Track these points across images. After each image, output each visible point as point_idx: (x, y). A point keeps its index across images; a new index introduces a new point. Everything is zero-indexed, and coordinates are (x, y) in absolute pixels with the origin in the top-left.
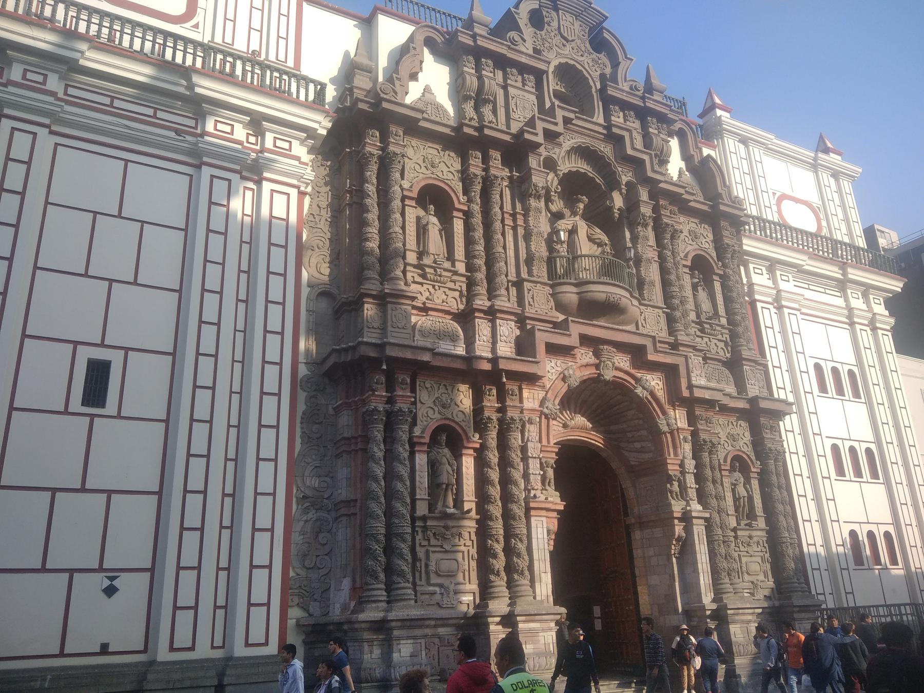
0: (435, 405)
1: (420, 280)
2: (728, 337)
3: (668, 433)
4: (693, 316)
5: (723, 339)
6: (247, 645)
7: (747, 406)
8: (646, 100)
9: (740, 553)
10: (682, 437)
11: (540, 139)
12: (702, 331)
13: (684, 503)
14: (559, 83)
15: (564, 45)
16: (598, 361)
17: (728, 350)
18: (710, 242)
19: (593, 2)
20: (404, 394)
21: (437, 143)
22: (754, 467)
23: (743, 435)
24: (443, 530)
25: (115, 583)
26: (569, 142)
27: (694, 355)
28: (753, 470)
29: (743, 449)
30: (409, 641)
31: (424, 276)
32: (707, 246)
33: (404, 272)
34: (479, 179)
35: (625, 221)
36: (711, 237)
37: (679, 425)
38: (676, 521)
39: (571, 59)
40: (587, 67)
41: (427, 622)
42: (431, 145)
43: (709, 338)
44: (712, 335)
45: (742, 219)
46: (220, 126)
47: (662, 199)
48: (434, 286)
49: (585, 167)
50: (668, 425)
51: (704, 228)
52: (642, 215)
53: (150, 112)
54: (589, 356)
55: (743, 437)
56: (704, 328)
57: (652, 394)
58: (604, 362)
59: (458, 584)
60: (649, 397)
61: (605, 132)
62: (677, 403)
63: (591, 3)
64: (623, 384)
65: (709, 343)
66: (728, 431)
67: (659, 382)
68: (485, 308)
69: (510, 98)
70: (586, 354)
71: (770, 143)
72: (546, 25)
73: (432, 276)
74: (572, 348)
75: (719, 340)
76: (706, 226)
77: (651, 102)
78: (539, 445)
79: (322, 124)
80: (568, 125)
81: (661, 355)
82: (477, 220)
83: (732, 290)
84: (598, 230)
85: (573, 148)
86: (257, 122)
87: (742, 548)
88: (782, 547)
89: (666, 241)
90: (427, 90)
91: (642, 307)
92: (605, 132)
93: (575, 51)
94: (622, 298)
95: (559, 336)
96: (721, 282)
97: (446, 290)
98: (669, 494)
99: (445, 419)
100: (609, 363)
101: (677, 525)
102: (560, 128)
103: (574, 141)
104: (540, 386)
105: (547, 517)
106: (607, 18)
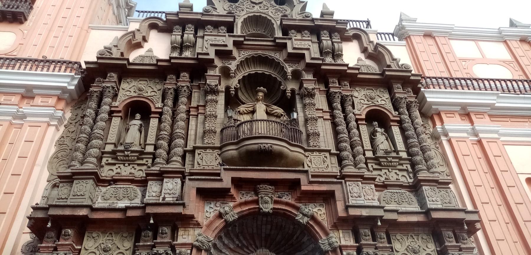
0: (98, 250)
4: (369, 154)
8: (315, 21)
11: (212, 56)
12: (379, 164)
15: (253, 7)
16: (256, 198)
17: (410, 177)
18: (386, 100)
20: (67, 243)
23: (427, 247)
27: (362, 183)
31: (116, 159)
32: (383, 102)
33: (100, 159)
34: (172, 91)
35: (297, 98)
36: (387, 96)
37: (343, 243)
39: (258, 12)
40: (270, 14)
43: (388, 169)
44: (389, 166)
47: (330, 77)
48: (124, 165)
50: (330, 244)
51: (380, 91)
54: (249, 195)
55: (426, 248)
56: (380, 162)
57: (313, 218)
58: (262, 198)
60: (311, 223)
64: (285, 213)
65: (388, 173)
66: (407, 244)
67: (321, 208)
69: (205, 41)
70: (247, 194)
71: (452, 30)
73: (122, 158)
74: (228, 190)
76: (382, 90)
77: (319, 21)
81: (315, 185)
82: (167, 117)
84: (275, 107)
85: (247, 59)
89: (335, 104)
90: (150, 51)
91: (307, 154)
93: (262, 7)
94: (274, 146)
97: (136, 166)
100: (267, 198)
102: (230, 47)
103: (246, 54)
104: (194, 225)
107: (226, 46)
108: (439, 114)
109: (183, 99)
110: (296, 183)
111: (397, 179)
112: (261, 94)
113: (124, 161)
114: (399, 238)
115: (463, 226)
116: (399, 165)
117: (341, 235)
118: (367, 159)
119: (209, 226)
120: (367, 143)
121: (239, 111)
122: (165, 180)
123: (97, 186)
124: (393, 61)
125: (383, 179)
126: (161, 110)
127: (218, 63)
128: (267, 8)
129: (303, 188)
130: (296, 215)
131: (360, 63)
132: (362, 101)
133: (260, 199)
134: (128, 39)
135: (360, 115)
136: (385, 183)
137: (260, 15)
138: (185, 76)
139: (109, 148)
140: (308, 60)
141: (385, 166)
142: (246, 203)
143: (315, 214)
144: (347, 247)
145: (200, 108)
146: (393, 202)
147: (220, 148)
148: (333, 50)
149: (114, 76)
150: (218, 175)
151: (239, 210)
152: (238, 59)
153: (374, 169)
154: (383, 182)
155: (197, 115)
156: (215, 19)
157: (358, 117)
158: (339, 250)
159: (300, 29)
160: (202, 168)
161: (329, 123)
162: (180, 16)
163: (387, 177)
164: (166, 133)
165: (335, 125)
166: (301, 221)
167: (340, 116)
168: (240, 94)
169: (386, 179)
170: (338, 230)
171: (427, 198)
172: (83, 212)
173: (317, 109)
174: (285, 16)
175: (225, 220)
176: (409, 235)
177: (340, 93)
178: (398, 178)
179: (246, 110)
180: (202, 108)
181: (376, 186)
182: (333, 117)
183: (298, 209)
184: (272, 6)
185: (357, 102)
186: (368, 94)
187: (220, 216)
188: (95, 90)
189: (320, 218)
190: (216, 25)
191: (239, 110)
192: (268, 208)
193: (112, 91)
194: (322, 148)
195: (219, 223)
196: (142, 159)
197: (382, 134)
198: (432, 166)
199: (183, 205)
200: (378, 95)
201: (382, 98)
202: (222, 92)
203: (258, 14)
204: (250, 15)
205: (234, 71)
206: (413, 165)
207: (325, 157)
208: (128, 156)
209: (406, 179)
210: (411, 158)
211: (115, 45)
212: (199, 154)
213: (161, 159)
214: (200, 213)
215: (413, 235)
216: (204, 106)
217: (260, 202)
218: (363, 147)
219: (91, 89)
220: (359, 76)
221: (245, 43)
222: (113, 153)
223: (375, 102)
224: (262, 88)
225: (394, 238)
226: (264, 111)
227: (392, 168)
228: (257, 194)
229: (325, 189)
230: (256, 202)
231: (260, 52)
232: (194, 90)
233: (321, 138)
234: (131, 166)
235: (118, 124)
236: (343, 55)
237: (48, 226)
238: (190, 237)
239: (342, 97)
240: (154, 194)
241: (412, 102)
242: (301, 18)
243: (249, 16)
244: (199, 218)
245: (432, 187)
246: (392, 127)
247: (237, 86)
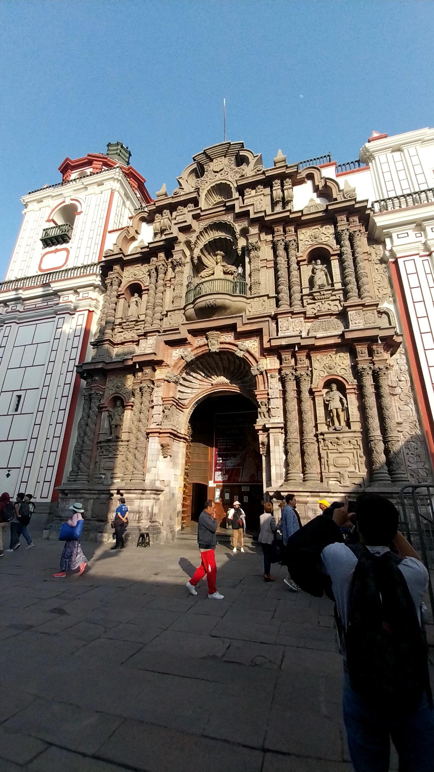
1: (122, 330)
2: (342, 296)
3: (259, 375)
4: (306, 291)
5: (337, 298)
6: (41, 497)
7: (339, 341)
9: (328, 451)
10: (269, 375)
12: (314, 299)
13: (269, 418)
14: (220, 197)
18: (330, 236)
19: (230, 141)
21: (138, 264)
22: (349, 385)
24: (108, 447)
25: (10, 473)
26: (197, 226)
27: (292, 318)
28: (347, 387)
29: (340, 374)
30: (74, 500)
31: (122, 328)
34: (154, 270)
37: (269, 367)
38: (260, 432)
39: (219, 180)
41: (81, 491)
42: (136, 266)
44: (323, 299)
45: (355, 207)
46: (65, 299)
49: (224, 234)
50: (258, 369)
52: (250, 244)
53: (46, 304)
54: (203, 341)
55: (341, 365)
57: (248, 352)
59: (113, 474)
61: (224, 208)
62: (265, 354)
63: (230, 143)
64: (228, 351)
66: (325, 363)
68: (143, 333)
72: (205, 172)
75: (332, 300)
76: (328, 226)
77: (270, 172)
78: (160, 398)
79: (97, 281)
80: (201, 218)
83: (345, 261)
85: (205, 228)
86: (75, 290)
87: (330, 446)
88: (370, 444)
91: (249, 301)
92: (224, 208)
93: (223, 174)
94: (217, 300)
95: (174, 335)
96: (338, 259)
98: (259, 415)
99: (116, 393)
101: (260, 434)
104: (165, 366)
105: (159, 437)
106: (242, 143)
107: (186, 222)
108: (391, 237)
109: (161, 276)
110: (232, 328)
111: (328, 309)
112: (219, 257)
113: (127, 329)
114: (318, 358)
115: (378, 342)
116: (331, 296)
117: (268, 362)
118: (302, 296)
119: (174, 366)
120: (305, 282)
121: (201, 276)
122: (148, 338)
123: (114, 348)
124: (339, 193)
125: (316, 311)
126: (147, 288)
127: (182, 237)
128: (227, 173)
129: (238, 330)
130: (236, 351)
131: (312, 203)
132: (307, 243)
133: (209, 342)
134: (124, 236)
135: (302, 256)
136: (316, 314)
137: (221, 183)
138: (162, 255)
139: (118, 321)
140: (252, 216)
141: (319, 300)
142: (200, 347)
143: (250, 349)
144: (271, 370)
145: (172, 280)
146: (321, 330)
147: (184, 309)
148: (283, 198)
149: (117, 268)
150: (178, 329)
151: (196, 352)
152: (198, 231)
153: (308, 304)
154: (315, 314)
155: (170, 286)
156: (182, 198)
157: (299, 259)
158: (264, 373)
159: (253, 185)
160: (171, 326)
161: (272, 270)
162: (157, 205)
163: (319, 309)
164: (151, 304)
165: (276, 271)
166: (238, 355)
167: (280, 262)
168: (205, 260)
169: (318, 311)
170: (266, 358)
171: (350, 322)
172: (100, 366)
173: (261, 260)
174: (243, 176)
175: (186, 361)
176: (328, 355)
177: (283, 240)
178: (330, 308)
179: (207, 274)
180: (174, 279)
181: (306, 318)
182: (276, 264)
183: (237, 346)
184: (232, 169)
185: (301, 245)
186: (313, 234)
187: (182, 358)
188: (108, 281)
189: (253, 352)
190: (184, 203)
191: (200, 275)
192: (215, 348)
193: (117, 280)
194: (261, 294)
195: (183, 363)
196: (138, 325)
197: (322, 270)
198: (364, 291)
199: (155, 354)
200: (323, 233)
201: (326, 235)
202: (188, 263)
203: (219, 182)
204: (212, 185)
205: (195, 243)
206: (346, 293)
207: (264, 301)
208: (128, 325)
209: (336, 308)
210: (344, 287)
211: (115, 243)
212: (170, 316)
213: (148, 324)
214: (169, 358)
215: (331, 355)
216: (175, 277)
217: (209, 345)
218: (301, 286)
219: (106, 282)
220: (303, 218)
221: (202, 214)
222: (120, 324)
223: (319, 241)
224: (219, 252)
225: (315, 359)
226: (221, 271)
227: (325, 300)
228: (207, 339)
229: (256, 328)
230: (207, 345)
231: (215, 219)
232: (169, 266)
233: (262, 286)
234: (132, 331)
235: (123, 304)
236: (292, 201)
237: (85, 375)
238: (163, 375)
239: (286, 243)
240: (143, 349)
241: (355, 232)
242: (254, 174)
243: (211, 187)
244: (167, 361)
245: (357, 311)
246: (332, 261)
247: (199, 255)
